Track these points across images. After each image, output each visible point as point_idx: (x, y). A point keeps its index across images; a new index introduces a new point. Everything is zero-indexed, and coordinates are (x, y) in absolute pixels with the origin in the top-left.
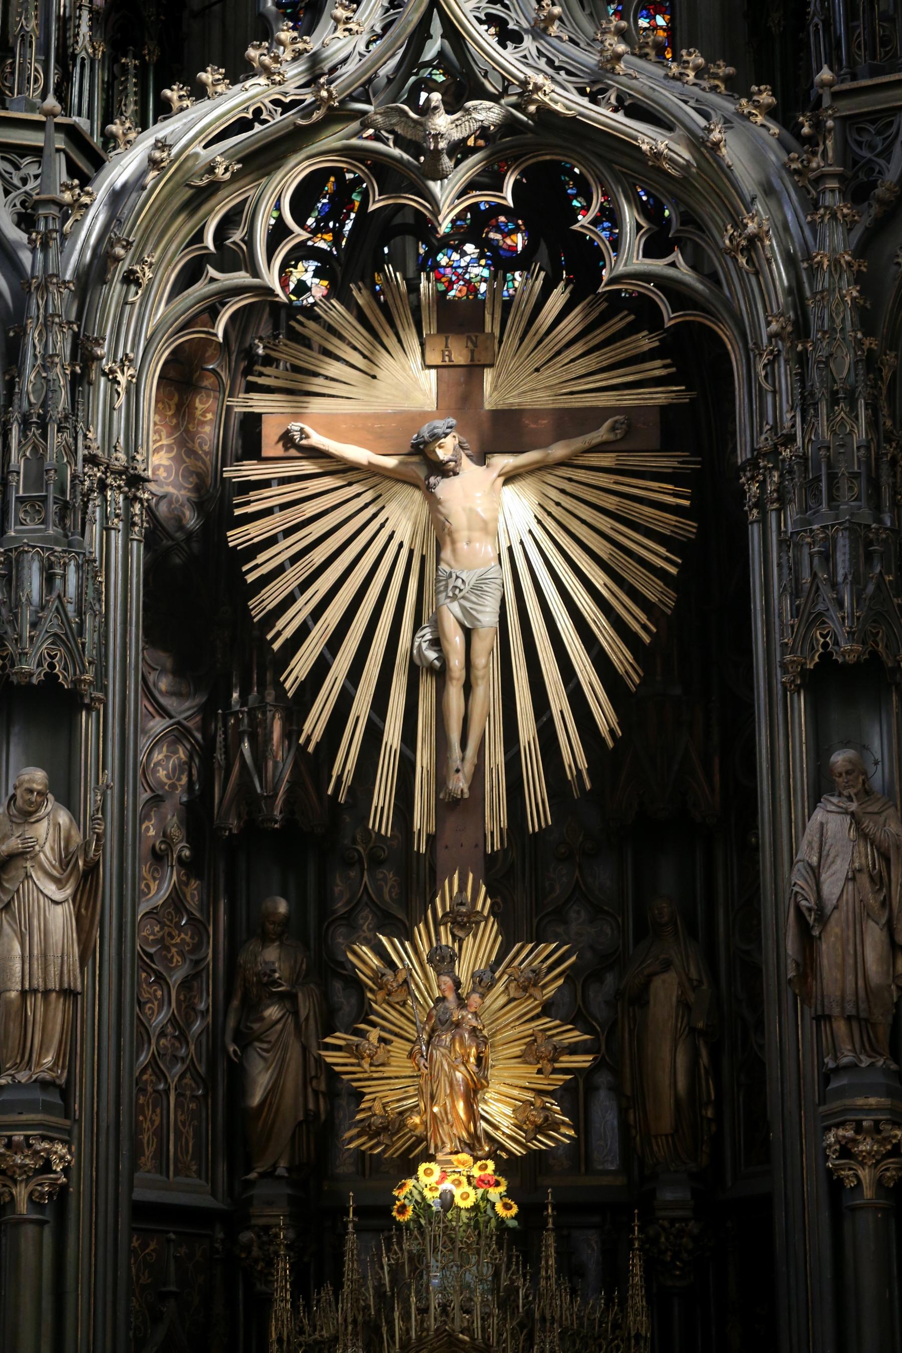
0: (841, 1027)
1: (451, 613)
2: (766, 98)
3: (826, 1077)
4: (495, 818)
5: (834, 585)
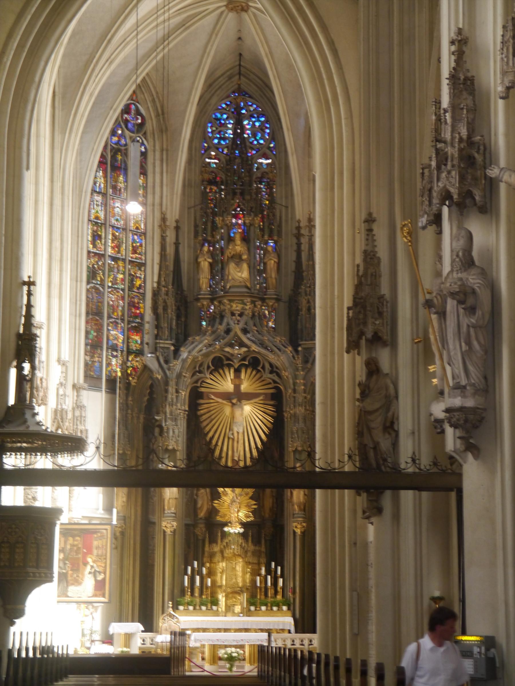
0: (296, 507)
1: (235, 429)
3: (294, 514)
4: (242, 464)
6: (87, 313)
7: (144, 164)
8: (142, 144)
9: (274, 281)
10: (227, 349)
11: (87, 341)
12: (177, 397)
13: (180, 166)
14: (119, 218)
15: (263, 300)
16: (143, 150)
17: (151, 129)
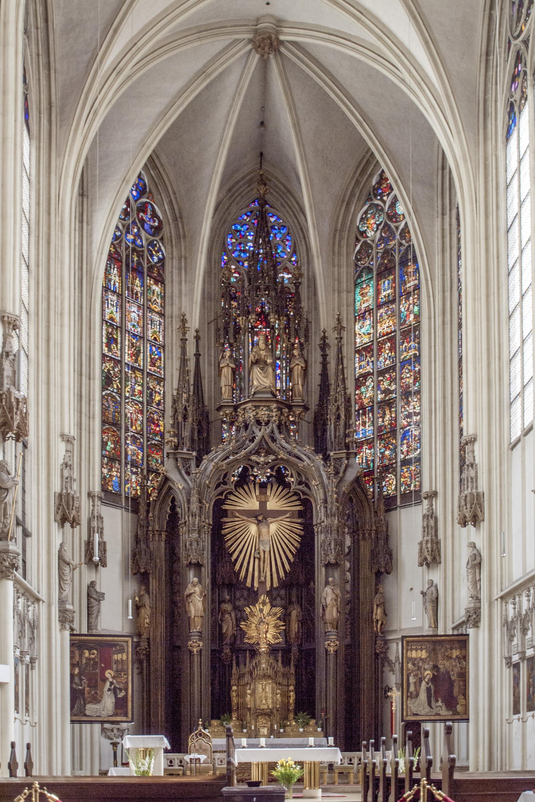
0: (329, 624)
2: (321, 457)
3: (326, 633)
5: (331, 549)
6: (104, 422)
7: (161, 272)
8: (160, 250)
9: (301, 388)
10: (254, 458)
11: (104, 452)
12: (201, 507)
13: (199, 271)
14: (136, 324)
15: (290, 407)
16: (161, 256)
17: (169, 235)
